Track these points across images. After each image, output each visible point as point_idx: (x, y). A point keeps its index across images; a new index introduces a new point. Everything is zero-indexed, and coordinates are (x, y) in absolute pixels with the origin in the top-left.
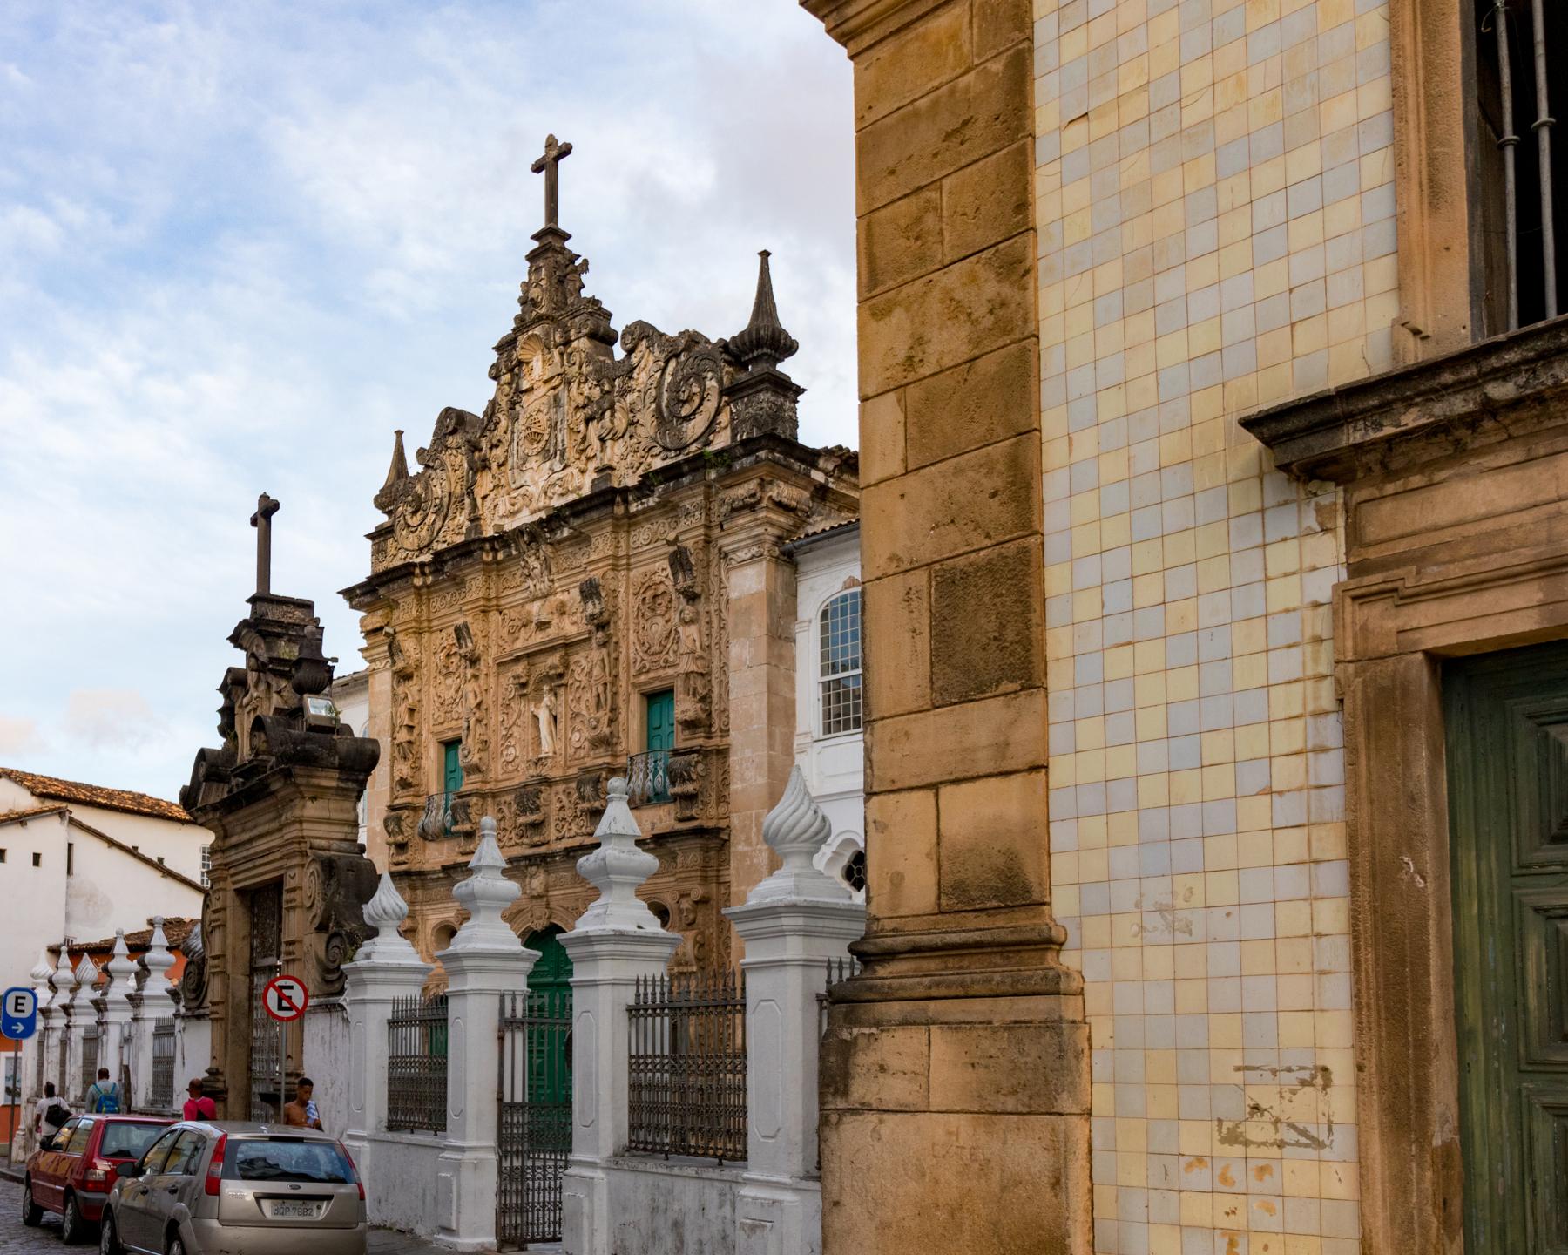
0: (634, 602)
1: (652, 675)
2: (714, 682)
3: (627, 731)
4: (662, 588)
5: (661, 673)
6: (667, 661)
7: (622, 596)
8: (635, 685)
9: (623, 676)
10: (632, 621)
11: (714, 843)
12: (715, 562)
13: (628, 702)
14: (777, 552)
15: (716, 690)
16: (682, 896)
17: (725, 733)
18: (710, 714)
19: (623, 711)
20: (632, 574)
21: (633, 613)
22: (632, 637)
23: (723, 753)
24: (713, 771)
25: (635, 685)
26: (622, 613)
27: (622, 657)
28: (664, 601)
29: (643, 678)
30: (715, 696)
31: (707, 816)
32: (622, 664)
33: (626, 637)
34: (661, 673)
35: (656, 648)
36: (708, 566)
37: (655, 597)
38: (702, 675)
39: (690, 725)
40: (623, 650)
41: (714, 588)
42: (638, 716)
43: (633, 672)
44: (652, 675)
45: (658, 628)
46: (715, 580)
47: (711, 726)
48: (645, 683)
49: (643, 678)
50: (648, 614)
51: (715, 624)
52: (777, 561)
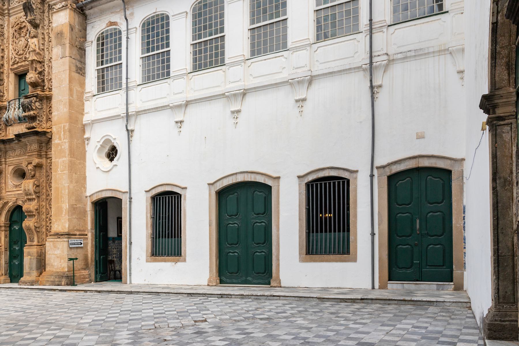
0: (12, 31)
1: (19, 64)
2: (46, 66)
3: (7, 90)
4: (24, 24)
5: (23, 63)
6: (25, 58)
7: (6, 28)
8: (11, 69)
9: (6, 65)
10: (11, 40)
11: (43, 139)
12: (46, 11)
13: (8, 77)
14: (75, 6)
15: (47, 69)
16: (29, 164)
17: (50, 90)
18: (43, 81)
19: (6, 81)
20: (11, 19)
21: (11, 35)
22: (11, 47)
23: (49, 98)
24: (45, 106)
25: (11, 69)
26: (6, 36)
27: (5, 56)
28: (24, 30)
29: (15, 66)
30: (46, 72)
31: (41, 126)
32: (5, 59)
33: (8, 47)
34: (23, 63)
35: (21, 52)
36: (43, 12)
37: (21, 28)
38: (40, 62)
39: (35, 85)
40: (6, 53)
41: (46, 22)
42: (13, 83)
43: (11, 63)
44: (19, 64)
45: (22, 42)
46: (46, 19)
47: (44, 86)
48: (16, 68)
49: (15, 66)
50: (18, 36)
51: (47, 39)
52: (74, 10)
